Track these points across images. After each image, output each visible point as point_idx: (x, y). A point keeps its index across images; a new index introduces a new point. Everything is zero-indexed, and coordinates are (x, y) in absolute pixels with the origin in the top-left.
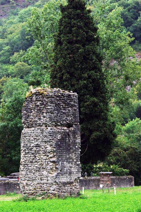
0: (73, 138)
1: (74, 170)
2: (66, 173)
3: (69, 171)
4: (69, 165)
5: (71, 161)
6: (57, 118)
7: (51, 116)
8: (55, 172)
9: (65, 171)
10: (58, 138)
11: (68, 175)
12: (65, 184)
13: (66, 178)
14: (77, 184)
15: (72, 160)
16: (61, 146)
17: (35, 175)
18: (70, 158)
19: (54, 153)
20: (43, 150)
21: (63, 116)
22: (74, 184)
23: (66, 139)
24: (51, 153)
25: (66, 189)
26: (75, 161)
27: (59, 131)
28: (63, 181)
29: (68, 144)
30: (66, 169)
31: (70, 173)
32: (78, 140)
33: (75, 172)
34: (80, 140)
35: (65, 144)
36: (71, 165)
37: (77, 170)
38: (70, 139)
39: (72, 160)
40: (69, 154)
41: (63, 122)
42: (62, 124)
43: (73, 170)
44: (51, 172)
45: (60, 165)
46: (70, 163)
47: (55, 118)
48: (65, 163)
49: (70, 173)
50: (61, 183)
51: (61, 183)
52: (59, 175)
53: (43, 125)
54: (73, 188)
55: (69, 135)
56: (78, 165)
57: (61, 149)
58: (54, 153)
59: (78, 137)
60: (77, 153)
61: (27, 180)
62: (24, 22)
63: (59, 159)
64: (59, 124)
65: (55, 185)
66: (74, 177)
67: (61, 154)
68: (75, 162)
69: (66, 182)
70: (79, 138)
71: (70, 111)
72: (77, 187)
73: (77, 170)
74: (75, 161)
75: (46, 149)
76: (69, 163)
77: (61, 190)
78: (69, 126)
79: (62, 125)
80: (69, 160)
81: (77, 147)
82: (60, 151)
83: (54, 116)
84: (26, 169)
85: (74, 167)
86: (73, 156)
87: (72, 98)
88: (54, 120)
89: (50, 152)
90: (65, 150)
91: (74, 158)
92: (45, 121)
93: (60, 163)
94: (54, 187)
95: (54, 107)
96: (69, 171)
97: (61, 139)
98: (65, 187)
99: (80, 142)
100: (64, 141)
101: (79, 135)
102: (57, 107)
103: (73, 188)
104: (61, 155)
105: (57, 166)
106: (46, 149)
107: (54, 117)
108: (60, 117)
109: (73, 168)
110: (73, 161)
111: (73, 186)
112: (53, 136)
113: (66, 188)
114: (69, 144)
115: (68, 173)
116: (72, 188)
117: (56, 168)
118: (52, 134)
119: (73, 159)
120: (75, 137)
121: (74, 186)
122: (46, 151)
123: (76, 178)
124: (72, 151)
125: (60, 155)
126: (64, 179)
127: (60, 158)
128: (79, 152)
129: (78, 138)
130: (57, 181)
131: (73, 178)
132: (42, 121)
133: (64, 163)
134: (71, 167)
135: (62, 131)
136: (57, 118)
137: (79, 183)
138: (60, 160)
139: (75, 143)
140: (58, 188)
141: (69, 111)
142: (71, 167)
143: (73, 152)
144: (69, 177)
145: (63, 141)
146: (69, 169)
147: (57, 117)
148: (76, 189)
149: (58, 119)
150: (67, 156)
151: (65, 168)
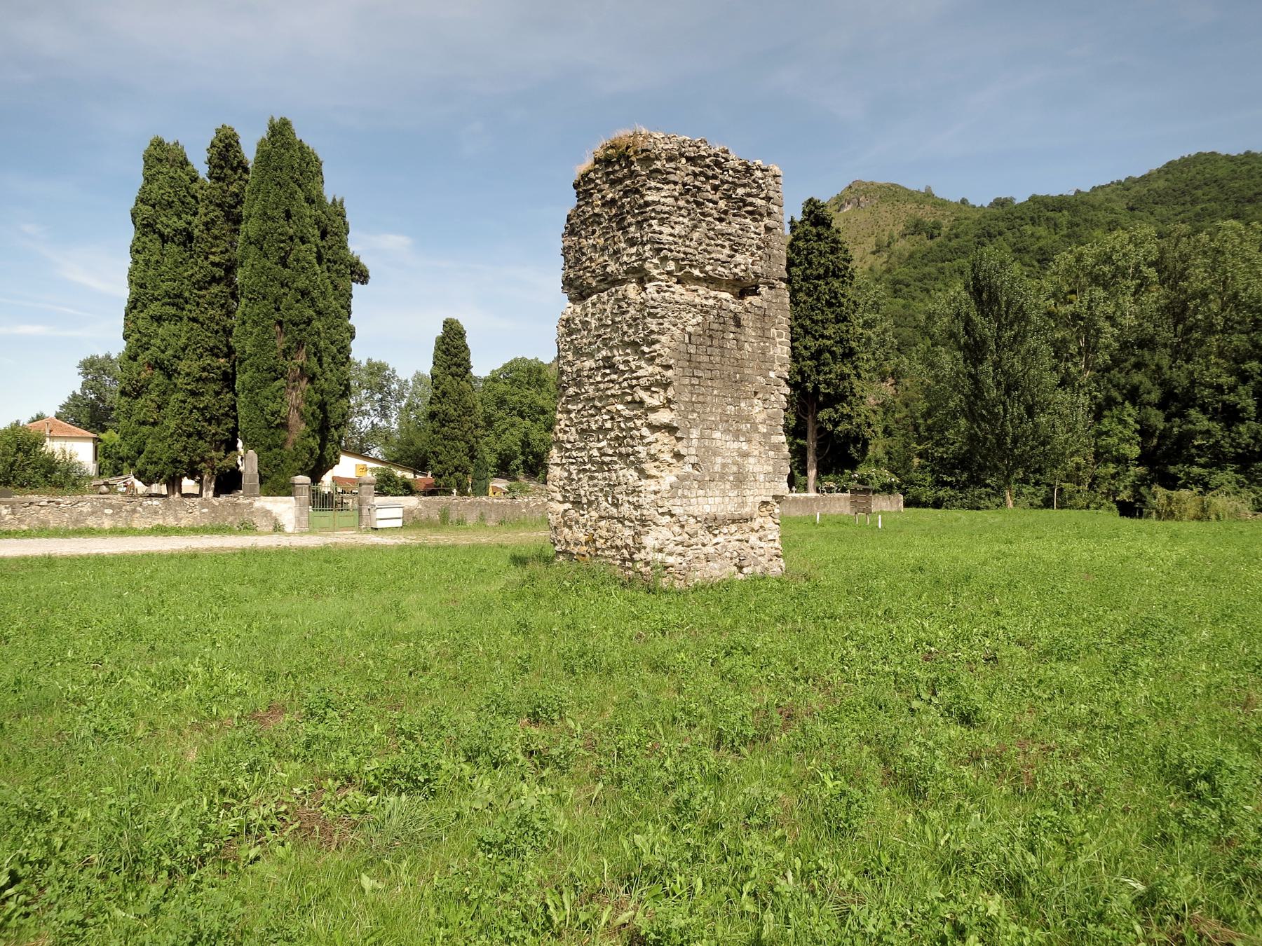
0: (755, 337)
1: (757, 469)
2: (723, 477)
3: (735, 469)
4: (736, 445)
5: (744, 429)
6: (689, 246)
7: (661, 233)
8: (671, 472)
9: (717, 468)
10: (689, 329)
11: (728, 486)
12: (712, 524)
13: (718, 500)
14: (769, 523)
15: (749, 425)
16: (699, 363)
17: (596, 481)
18: (740, 417)
19: (665, 390)
20: (625, 380)
21: (717, 245)
22: (756, 525)
23: (723, 338)
24: (653, 389)
25: (717, 544)
26: (763, 429)
27: (697, 300)
28: (707, 509)
29: (732, 360)
30: (719, 460)
31: (740, 480)
32: (779, 350)
33: (762, 476)
34: (786, 348)
35: (718, 359)
36: (745, 446)
37: (770, 469)
38: (743, 338)
39: (749, 425)
40: (736, 402)
41: (713, 270)
42: (711, 273)
43: (751, 465)
44: (654, 472)
45: (695, 442)
46: (742, 439)
47: (676, 243)
48: (717, 435)
49: (740, 480)
50: (695, 518)
51: (695, 518)
52: (688, 483)
53: (630, 276)
54: (753, 538)
55: (738, 324)
56: (776, 447)
57: (697, 377)
58: (665, 390)
59: (780, 335)
60: (773, 398)
61: (571, 499)
62: (724, 224)
63: (690, 417)
64: (696, 272)
65: (668, 526)
66: (756, 493)
67: (701, 398)
68: (764, 435)
69: (721, 514)
70: (783, 339)
71: (747, 232)
72: (770, 537)
73: (770, 469)
74: (763, 429)
75: (634, 375)
76: (737, 435)
77: (694, 547)
78: (744, 289)
79: (710, 281)
80: (738, 425)
81: (772, 374)
82: (693, 385)
83: (671, 235)
84: (569, 457)
85: (756, 453)
86: (757, 410)
87: (761, 181)
88: (671, 251)
89: (651, 385)
90: (716, 383)
91: (760, 418)
92: (634, 258)
93: (695, 433)
94: (661, 537)
95: (676, 199)
96: (735, 469)
97: (700, 335)
98: (715, 535)
99: (786, 356)
100: (715, 342)
101: (785, 329)
102: (688, 202)
103: (753, 538)
104: (699, 402)
105: (681, 447)
106: (634, 375)
107: (671, 238)
108: (700, 244)
109: (752, 460)
110: (756, 430)
111: (752, 530)
112: (663, 317)
113: (720, 539)
114: (737, 360)
115: (731, 478)
116: (747, 542)
117: (678, 456)
118: (659, 310)
119: (754, 423)
120: (764, 335)
121: (757, 531)
122: (634, 382)
123: (765, 499)
124: (750, 388)
125: (693, 403)
126: (711, 500)
127: (695, 415)
128: (783, 398)
129: (778, 340)
130: (676, 510)
131: (750, 499)
132: (625, 258)
133: (714, 436)
134: (746, 455)
135: (711, 302)
136: (689, 246)
137: (777, 521)
138: (693, 424)
139: (764, 359)
140: (678, 539)
141: (744, 229)
142: (746, 455)
143: (756, 393)
144: (733, 494)
145: (709, 343)
146: (733, 463)
147: (688, 243)
148: (762, 544)
149: (691, 251)
150: (729, 407)
151: (715, 454)
